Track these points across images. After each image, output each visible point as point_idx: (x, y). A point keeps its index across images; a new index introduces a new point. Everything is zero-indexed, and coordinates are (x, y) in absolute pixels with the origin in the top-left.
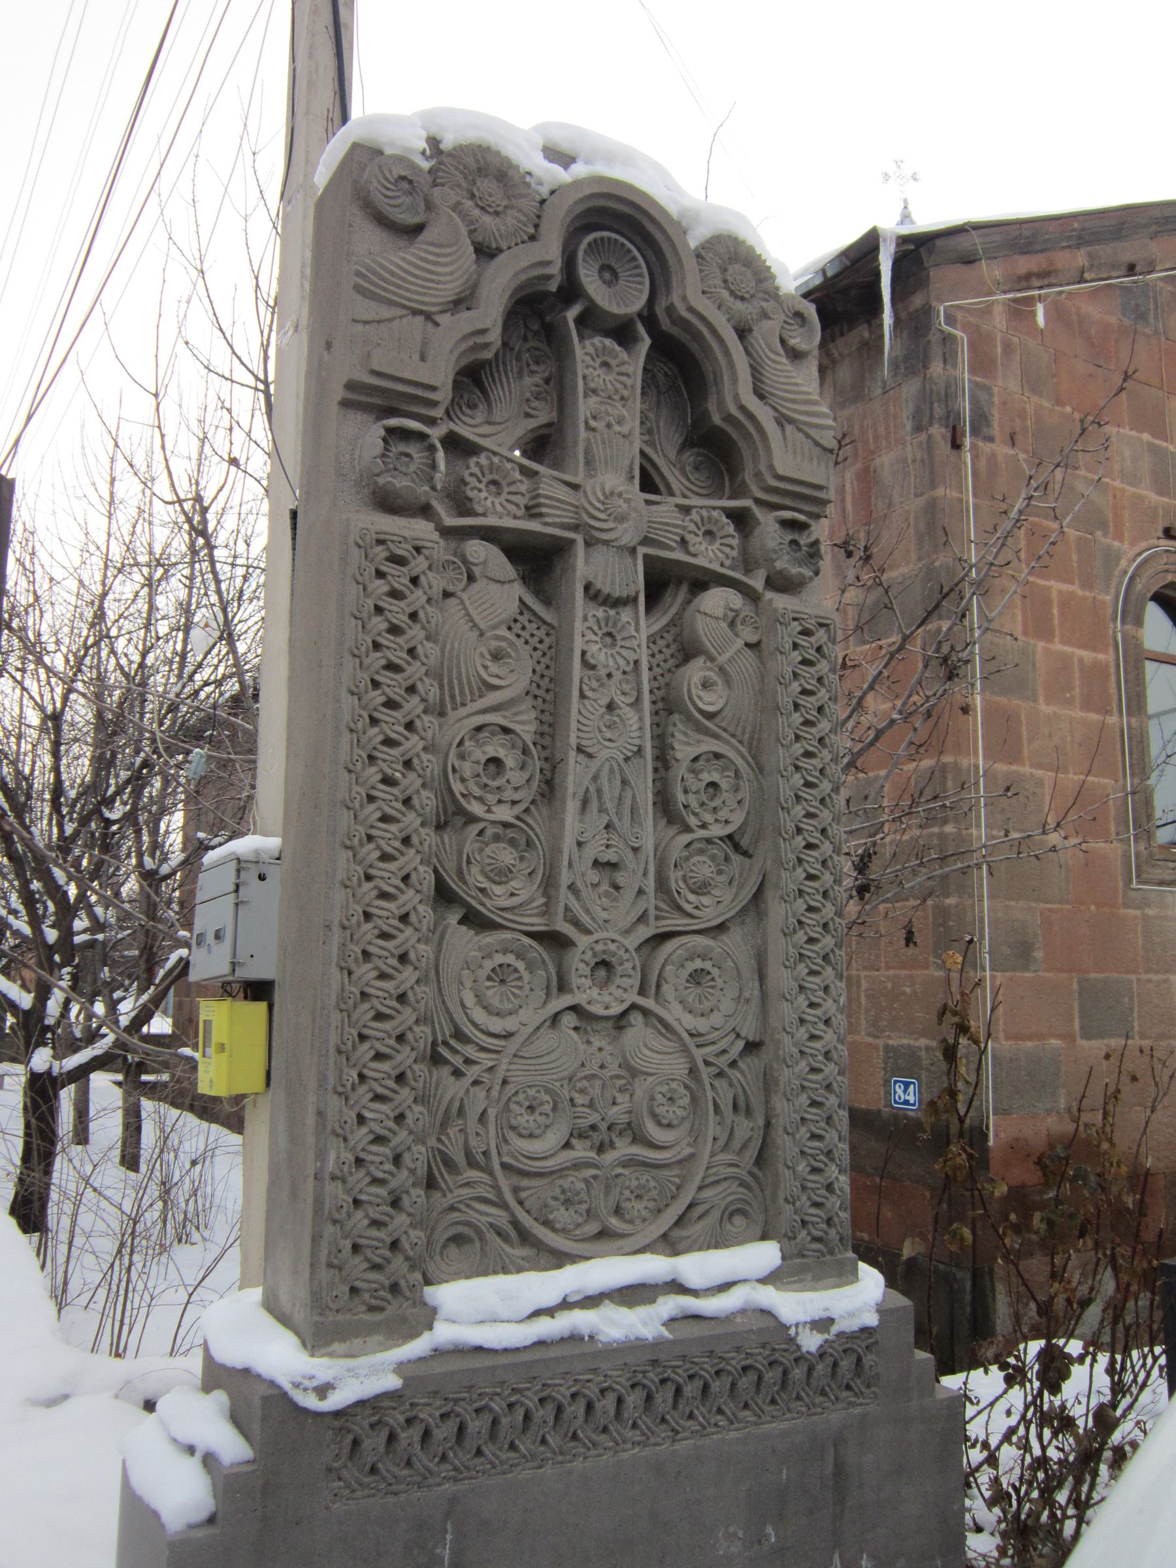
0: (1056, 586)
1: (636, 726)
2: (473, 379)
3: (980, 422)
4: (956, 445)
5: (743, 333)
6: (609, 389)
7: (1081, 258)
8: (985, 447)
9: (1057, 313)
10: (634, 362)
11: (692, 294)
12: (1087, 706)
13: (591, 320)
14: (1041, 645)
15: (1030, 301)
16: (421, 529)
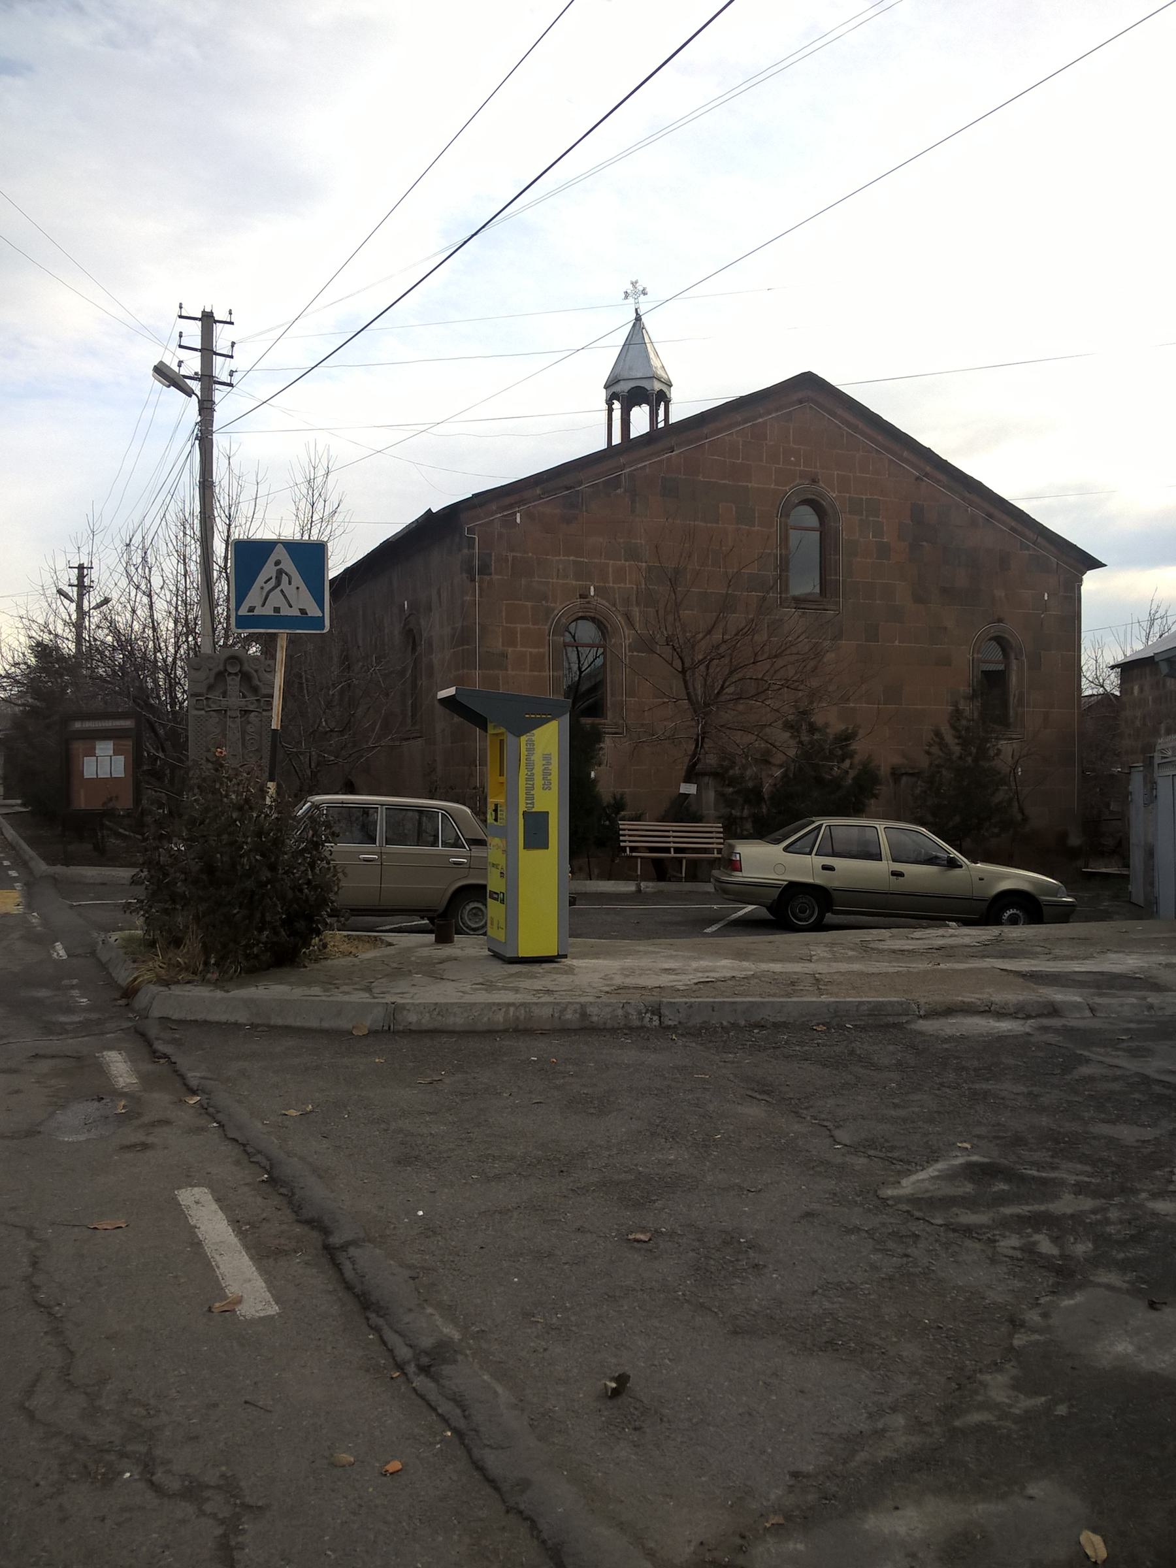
0: (519, 626)
1: (239, 735)
2: (210, 688)
3: (484, 569)
4: (473, 580)
5: (256, 671)
6: (233, 683)
7: (538, 491)
8: (487, 578)
9: (528, 516)
10: (238, 679)
11: (246, 668)
12: (531, 670)
13: (230, 674)
14: (510, 650)
15: (515, 514)
16: (203, 712)
